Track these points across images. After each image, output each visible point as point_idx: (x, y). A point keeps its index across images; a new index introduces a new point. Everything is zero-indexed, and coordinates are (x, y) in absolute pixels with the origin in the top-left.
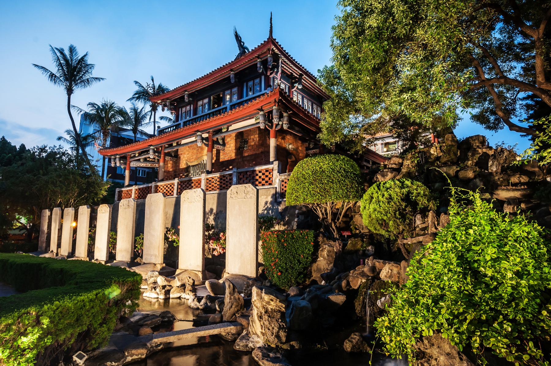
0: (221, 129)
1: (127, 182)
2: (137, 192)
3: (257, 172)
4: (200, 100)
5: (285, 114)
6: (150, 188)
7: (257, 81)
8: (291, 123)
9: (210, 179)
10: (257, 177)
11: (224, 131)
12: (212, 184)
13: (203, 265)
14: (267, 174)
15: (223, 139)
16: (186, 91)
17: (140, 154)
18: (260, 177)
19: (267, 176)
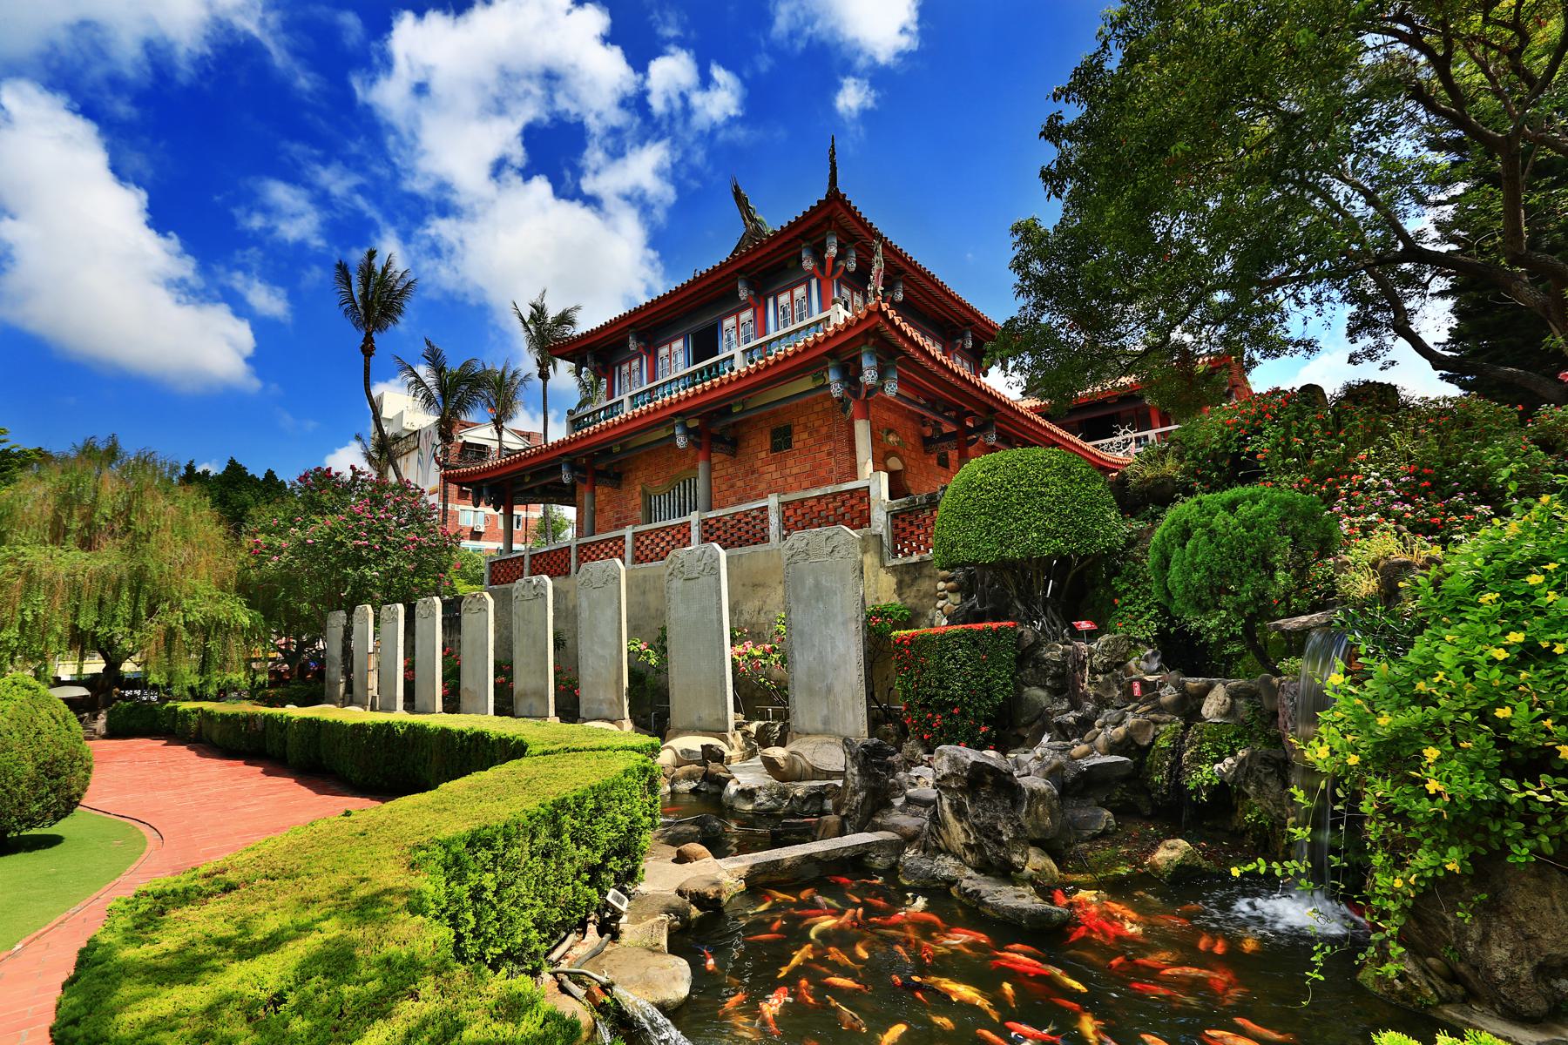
0: (729, 407)
4: (663, 345)
7: (800, 292)
11: (736, 409)
17: (534, 476)
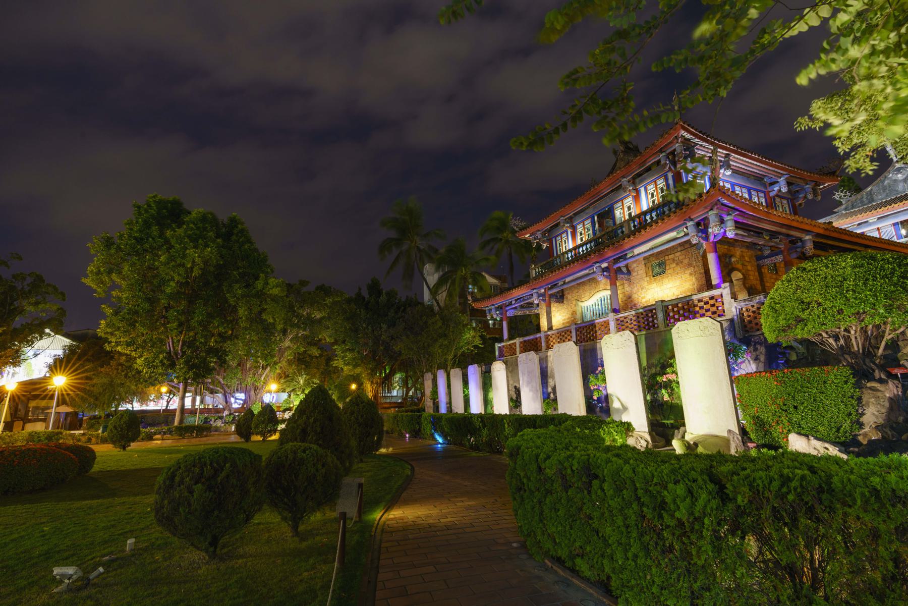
0: (626, 255)
1: (506, 336)
2: (522, 345)
3: (696, 302)
5: (727, 218)
6: (539, 339)
8: (738, 225)
9: (621, 319)
10: (697, 309)
12: (626, 325)
13: (648, 424)
14: (712, 302)
15: (627, 266)
16: (562, 216)
18: (701, 308)
19: (713, 305)
